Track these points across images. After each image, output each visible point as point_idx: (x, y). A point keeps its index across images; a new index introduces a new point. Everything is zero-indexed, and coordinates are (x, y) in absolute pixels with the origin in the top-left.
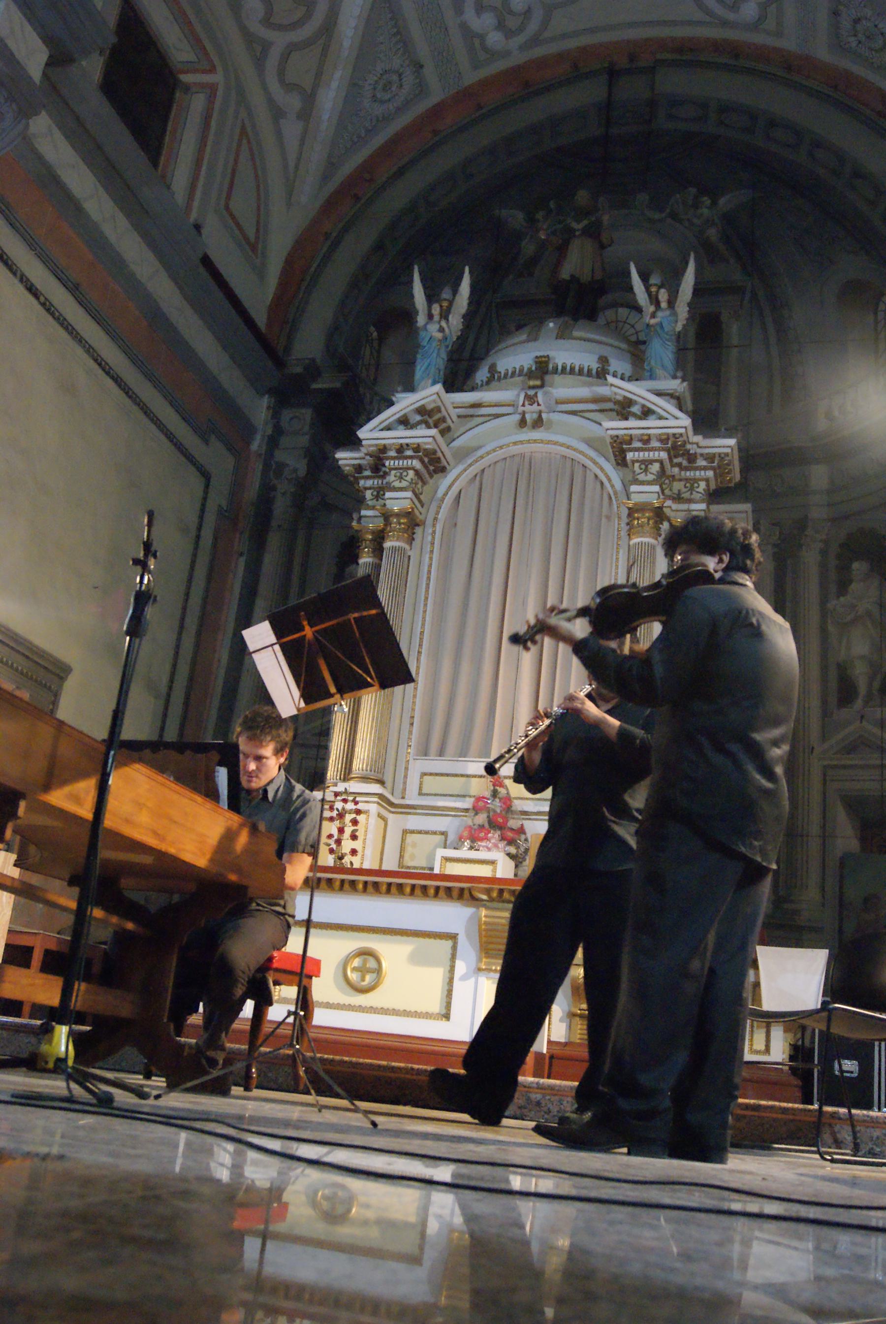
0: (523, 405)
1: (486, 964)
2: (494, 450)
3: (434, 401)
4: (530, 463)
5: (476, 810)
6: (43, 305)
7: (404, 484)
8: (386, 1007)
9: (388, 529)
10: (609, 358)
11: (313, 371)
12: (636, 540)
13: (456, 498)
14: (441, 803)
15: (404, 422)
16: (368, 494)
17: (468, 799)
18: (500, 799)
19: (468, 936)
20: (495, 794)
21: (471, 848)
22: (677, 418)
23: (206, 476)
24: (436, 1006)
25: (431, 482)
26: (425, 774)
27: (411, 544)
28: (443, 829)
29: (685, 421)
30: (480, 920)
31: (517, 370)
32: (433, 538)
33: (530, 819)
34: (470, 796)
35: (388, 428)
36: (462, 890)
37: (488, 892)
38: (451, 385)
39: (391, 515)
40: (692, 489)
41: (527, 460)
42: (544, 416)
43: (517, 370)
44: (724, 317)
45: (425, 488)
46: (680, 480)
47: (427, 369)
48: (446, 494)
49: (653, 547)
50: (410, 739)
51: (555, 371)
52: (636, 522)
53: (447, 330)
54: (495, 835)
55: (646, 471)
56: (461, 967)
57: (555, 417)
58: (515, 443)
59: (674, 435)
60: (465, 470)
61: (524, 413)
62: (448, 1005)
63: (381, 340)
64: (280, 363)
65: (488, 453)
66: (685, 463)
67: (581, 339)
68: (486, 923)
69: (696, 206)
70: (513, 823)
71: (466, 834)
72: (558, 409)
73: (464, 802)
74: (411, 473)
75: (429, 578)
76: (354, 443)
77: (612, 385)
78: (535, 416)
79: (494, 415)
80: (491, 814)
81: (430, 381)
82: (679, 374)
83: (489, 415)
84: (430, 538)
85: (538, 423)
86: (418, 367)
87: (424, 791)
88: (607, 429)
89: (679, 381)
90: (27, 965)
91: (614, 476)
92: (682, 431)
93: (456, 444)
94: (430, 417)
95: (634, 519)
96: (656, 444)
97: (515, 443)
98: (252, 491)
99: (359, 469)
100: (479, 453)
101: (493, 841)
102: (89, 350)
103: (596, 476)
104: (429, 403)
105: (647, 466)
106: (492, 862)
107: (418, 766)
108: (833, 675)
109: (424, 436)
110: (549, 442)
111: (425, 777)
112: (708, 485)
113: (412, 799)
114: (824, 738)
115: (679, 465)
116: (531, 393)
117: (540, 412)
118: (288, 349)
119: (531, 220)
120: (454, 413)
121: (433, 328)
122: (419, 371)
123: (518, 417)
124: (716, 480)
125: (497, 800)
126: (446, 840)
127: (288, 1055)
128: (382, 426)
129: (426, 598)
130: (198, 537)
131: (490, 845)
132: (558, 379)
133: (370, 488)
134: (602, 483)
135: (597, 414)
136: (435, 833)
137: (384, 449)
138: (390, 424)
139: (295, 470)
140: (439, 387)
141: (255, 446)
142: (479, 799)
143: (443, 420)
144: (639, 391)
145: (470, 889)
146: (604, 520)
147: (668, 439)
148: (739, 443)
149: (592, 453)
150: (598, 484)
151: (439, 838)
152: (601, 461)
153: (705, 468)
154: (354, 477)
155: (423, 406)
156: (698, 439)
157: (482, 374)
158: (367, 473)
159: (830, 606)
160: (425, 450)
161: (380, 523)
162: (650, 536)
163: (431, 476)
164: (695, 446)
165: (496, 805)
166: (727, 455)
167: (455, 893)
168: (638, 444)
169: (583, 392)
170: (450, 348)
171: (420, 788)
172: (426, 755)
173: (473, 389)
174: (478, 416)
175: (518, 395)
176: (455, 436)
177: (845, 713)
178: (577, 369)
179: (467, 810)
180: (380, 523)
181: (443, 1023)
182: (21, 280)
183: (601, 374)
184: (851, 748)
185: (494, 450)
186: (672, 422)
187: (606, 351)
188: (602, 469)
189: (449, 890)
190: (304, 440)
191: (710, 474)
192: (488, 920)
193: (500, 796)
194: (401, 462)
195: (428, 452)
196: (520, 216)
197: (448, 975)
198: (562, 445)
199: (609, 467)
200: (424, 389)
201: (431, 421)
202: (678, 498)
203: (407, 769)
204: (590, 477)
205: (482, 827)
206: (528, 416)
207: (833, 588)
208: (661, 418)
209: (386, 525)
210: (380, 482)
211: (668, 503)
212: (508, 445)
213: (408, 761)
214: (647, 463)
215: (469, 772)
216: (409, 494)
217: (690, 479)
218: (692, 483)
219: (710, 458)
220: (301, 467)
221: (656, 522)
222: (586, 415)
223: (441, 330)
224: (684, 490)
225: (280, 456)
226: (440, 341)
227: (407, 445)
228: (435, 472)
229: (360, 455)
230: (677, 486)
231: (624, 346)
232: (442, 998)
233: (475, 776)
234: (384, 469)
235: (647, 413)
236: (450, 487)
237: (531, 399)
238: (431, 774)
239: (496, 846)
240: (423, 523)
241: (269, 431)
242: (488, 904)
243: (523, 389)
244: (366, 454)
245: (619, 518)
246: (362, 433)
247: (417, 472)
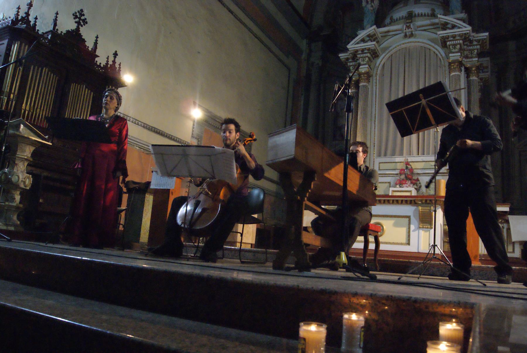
0: (405, 30)
1: (422, 225)
2: (396, 47)
3: (373, 32)
4: (409, 50)
5: (401, 174)
6: (234, 16)
7: (365, 62)
8: (386, 241)
9: (361, 79)
10: (435, 9)
12: (453, 74)
13: (382, 67)
14: (387, 172)
15: (363, 41)
16: (351, 68)
17: (396, 170)
18: (409, 169)
19: (414, 216)
20: (407, 168)
21: (400, 187)
22: (466, 27)
23: (289, 69)
24: (404, 241)
25: (373, 61)
26: (380, 163)
27: (368, 83)
28: (389, 181)
29: (469, 28)
30: (419, 211)
31: (401, 17)
32: (376, 81)
33: (420, 176)
34: (397, 169)
35: (358, 43)
36: (411, 201)
37: (421, 201)
38: (379, 27)
39: (361, 74)
40: (472, 53)
41: (408, 50)
42: (413, 33)
43: (401, 17)
45: (372, 63)
46: (467, 50)
47: (368, 21)
48: (379, 64)
49: (459, 76)
50: (374, 151)
51: (415, 16)
52: (452, 67)
53: (374, 6)
54: (409, 182)
55: (455, 48)
56: (412, 227)
57: (416, 32)
58: (403, 44)
59: (465, 34)
60: (386, 55)
61: (406, 32)
62: (409, 240)
65: (394, 49)
66: (469, 44)
67: (424, 3)
68: (422, 212)
70: (415, 177)
71: (398, 182)
72: (418, 30)
73: (395, 171)
74: (367, 59)
75: (376, 95)
76: (346, 50)
77: (439, 18)
78: (410, 33)
79: (394, 35)
80: (406, 175)
81: (369, 26)
82: (464, 11)
83: (393, 35)
84: (375, 81)
85: (412, 35)
86: (365, 21)
87: (381, 168)
88: (439, 35)
89: (464, 14)
91: (441, 52)
92: (468, 32)
93: (382, 46)
94: (372, 37)
95: (452, 66)
96: (458, 38)
97: (403, 44)
98: (304, 72)
99: (347, 59)
100: (390, 49)
101: (408, 184)
102: (250, 30)
103: (434, 52)
104: (372, 33)
105: (455, 46)
106: (410, 191)
107: (378, 160)
109: (370, 45)
110: (416, 42)
111: (381, 164)
112: (478, 51)
115: (467, 45)
116: (408, 25)
117: (412, 31)
120: (380, 35)
121: (369, 6)
122: (365, 23)
123: (403, 35)
124: (480, 50)
125: (408, 170)
126: (390, 185)
127: (372, 259)
128: (355, 43)
129: (376, 102)
130: (288, 90)
131: (407, 185)
132: (417, 18)
133: (352, 66)
134: (437, 55)
135: (433, 29)
136: (386, 183)
137: (357, 51)
138: (358, 42)
139: (318, 64)
140: (374, 27)
142: (402, 170)
143: (376, 38)
144: (450, 19)
145: (414, 201)
146: (439, 68)
147: (463, 35)
148: (489, 34)
149: (433, 44)
150: (435, 55)
151: (387, 184)
152: (436, 47)
153: (476, 45)
154: (346, 62)
155: (370, 34)
156: (474, 34)
157: (388, 21)
158: (350, 60)
160: (372, 49)
161: (357, 77)
162: (458, 72)
163: (374, 59)
164: (473, 37)
166: (485, 39)
167: (409, 202)
168: (452, 39)
169: (428, 22)
170: (376, 12)
171: (379, 168)
172: (385, 156)
173: (384, 26)
174: (389, 35)
175: (403, 26)
176: (381, 43)
178: (423, 14)
179: (397, 174)
180: (357, 77)
181: (408, 246)
182: (227, 9)
183: (433, 15)
185: (396, 47)
186: (464, 29)
188: (436, 49)
189: (406, 201)
191: (478, 47)
192: (422, 210)
193: (409, 168)
194: (363, 55)
195: (372, 50)
197: (408, 230)
198: (421, 42)
199: (439, 49)
200: (368, 28)
201: (372, 39)
202: (467, 57)
203: (374, 161)
204: (432, 53)
205: (403, 180)
206: (407, 33)
208: (459, 28)
209: (359, 78)
210: (355, 63)
211: (464, 59)
212: (400, 45)
213: (374, 159)
214: (454, 45)
215: (396, 161)
216: (367, 66)
217: (471, 50)
218: (471, 51)
219: (478, 41)
221: (460, 67)
222: (428, 30)
223: (372, 6)
224: (469, 54)
226: (372, 10)
227: (365, 48)
228: (375, 57)
229: (348, 54)
230: (466, 53)
231: (439, 4)
232: (406, 238)
233: (398, 162)
234: (356, 58)
235: (454, 27)
236: (381, 62)
237: (409, 27)
238: (382, 163)
239: (410, 186)
240: (372, 76)
242: (422, 205)
243: (405, 24)
244: (350, 54)
245: (445, 67)
246: (349, 46)
247: (369, 58)
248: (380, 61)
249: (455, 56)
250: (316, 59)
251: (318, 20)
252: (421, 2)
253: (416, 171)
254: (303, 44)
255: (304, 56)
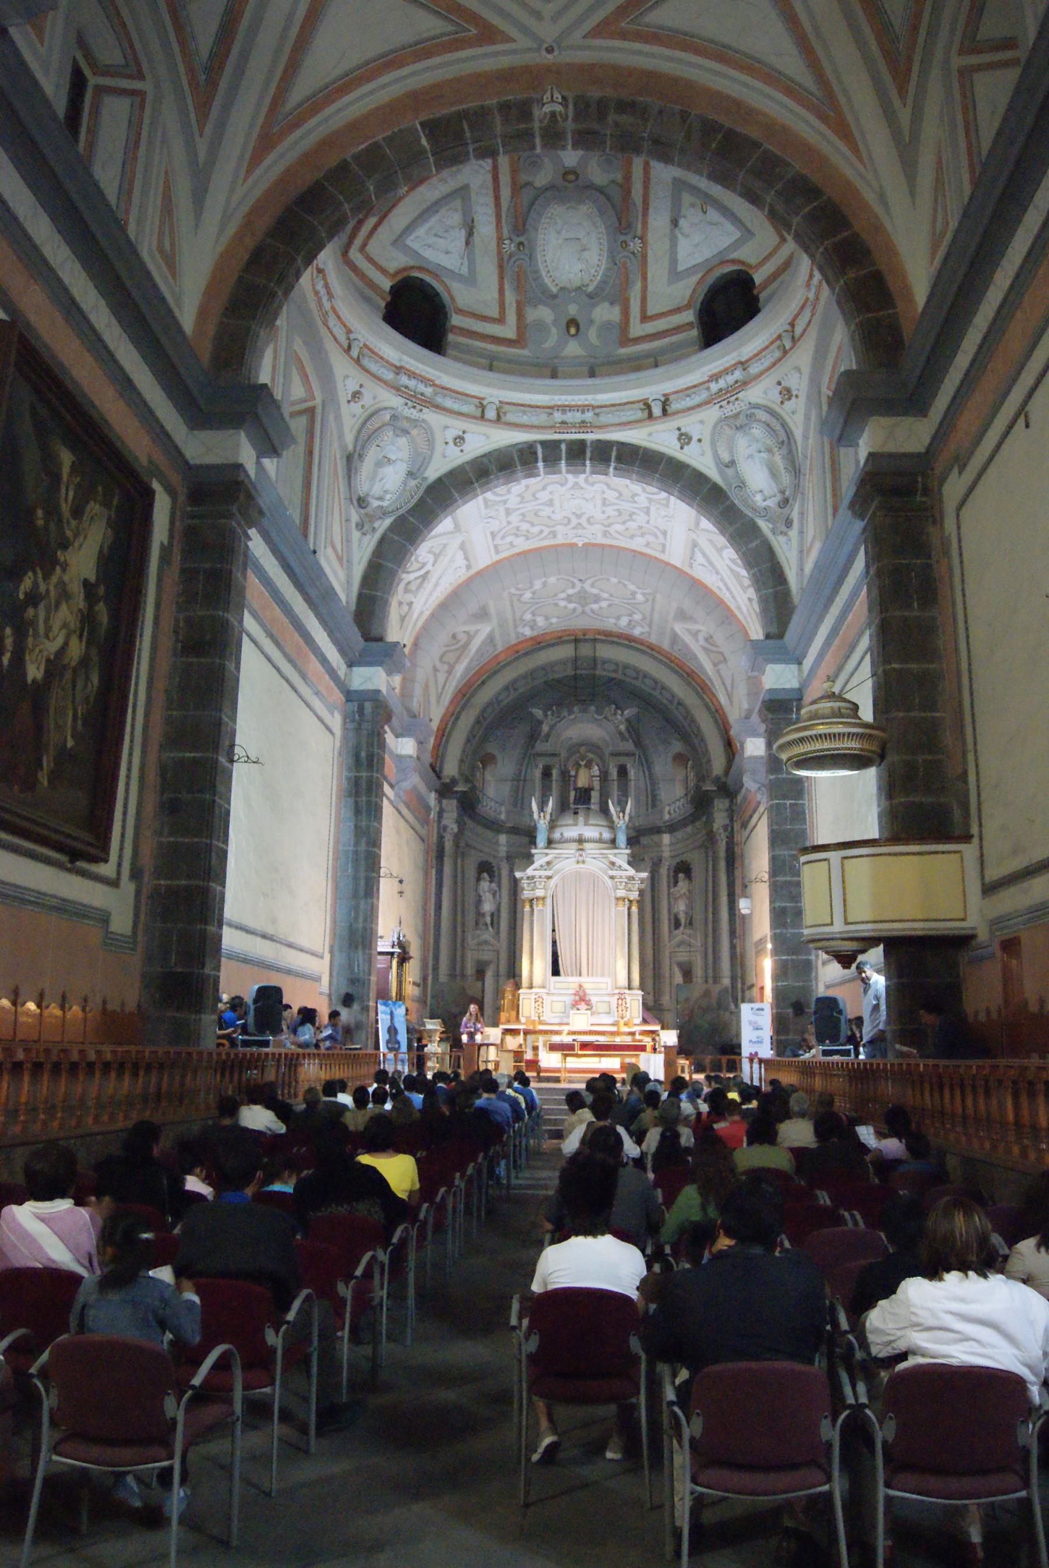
5: (575, 995)
11: (454, 781)
44: (629, 766)
63: (484, 768)
64: (439, 777)
69: (615, 714)
85: (583, 862)
90: (516, 1061)
108: (672, 917)
113: (553, 991)
114: (670, 941)
118: (441, 767)
119: (546, 716)
123: (574, 860)
141: (432, 816)
159: (672, 890)
165: (581, 994)
177: (677, 931)
184: (679, 946)
187: (602, 829)
190: (455, 815)
196: (541, 712)
207: (672, 884)
220: (455, 828)
225: (444, 822)
241: (438, 809)
248: (552, 883)
249: (621, 893)
250: (450, 821)
251: (451, 769)
252: (591, 822)
253: (588, 992)
254: (432, 798)
255: (433, 815)
